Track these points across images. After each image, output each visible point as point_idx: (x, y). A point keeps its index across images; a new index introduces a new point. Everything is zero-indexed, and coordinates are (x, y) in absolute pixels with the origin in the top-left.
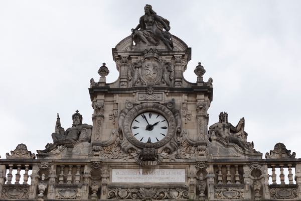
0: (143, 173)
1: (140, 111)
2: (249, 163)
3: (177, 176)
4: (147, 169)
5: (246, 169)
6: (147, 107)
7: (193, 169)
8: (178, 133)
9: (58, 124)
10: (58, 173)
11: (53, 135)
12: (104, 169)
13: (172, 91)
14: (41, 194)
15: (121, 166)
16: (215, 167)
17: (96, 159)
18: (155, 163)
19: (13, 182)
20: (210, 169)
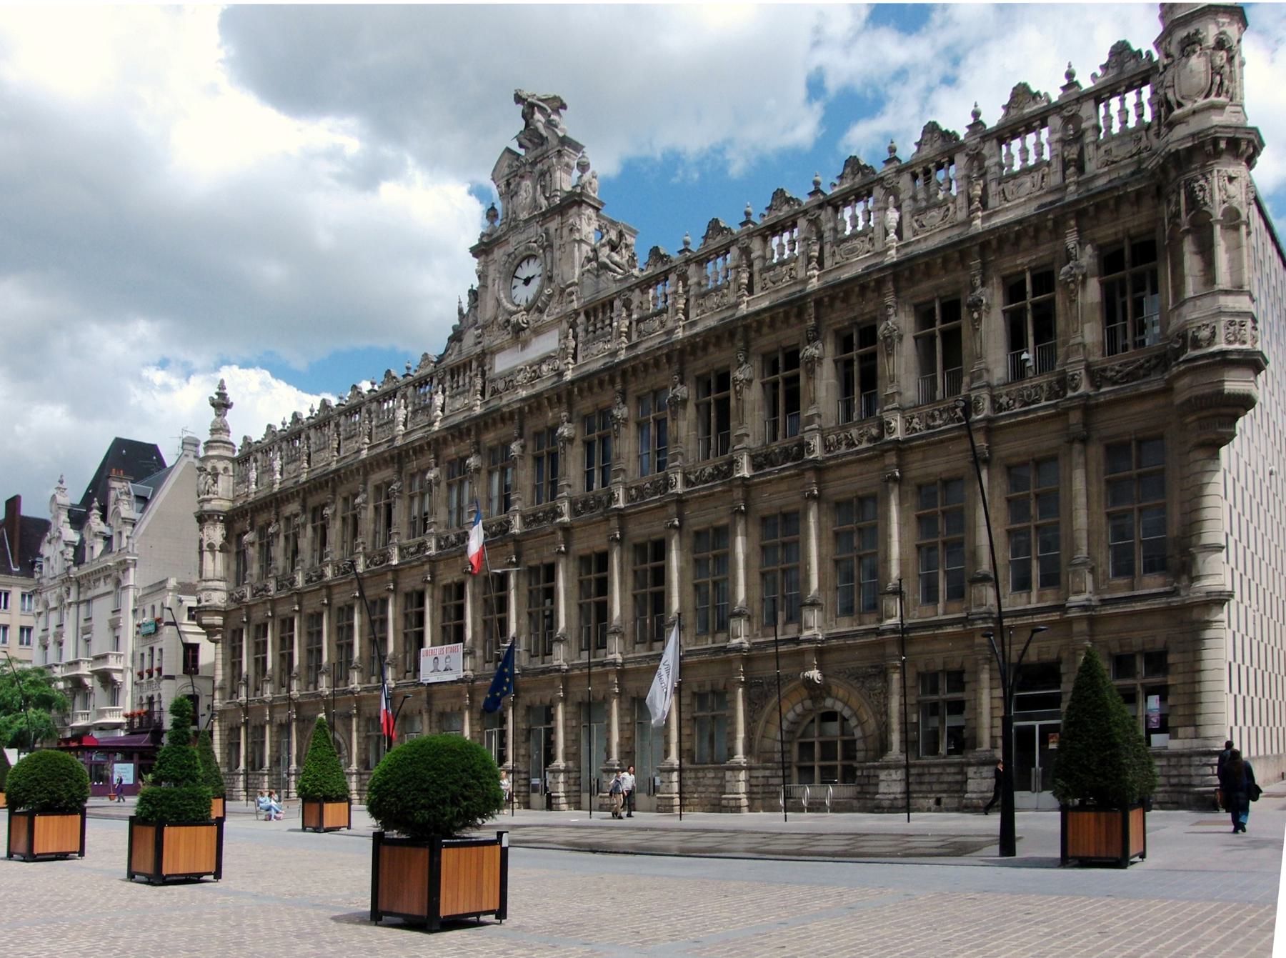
0: (523, 348)
1: (516, 262)
2: (619, 294)
3: (547, 343)
4: (525, 345)
5: (617, 303)
6: (521, 254)
7: (565, 325)
8: (550, 279)
9: (460, 311)
10: (453, 378)
11: (454, 328)
12: (487, 359)
13: (546, 216)
14: (977, 204)
15: (501, 349)
16: (587, 315)
17: (478, 349)
18: (528, 332)
19: (1116, 129)
20: (582, 318)
